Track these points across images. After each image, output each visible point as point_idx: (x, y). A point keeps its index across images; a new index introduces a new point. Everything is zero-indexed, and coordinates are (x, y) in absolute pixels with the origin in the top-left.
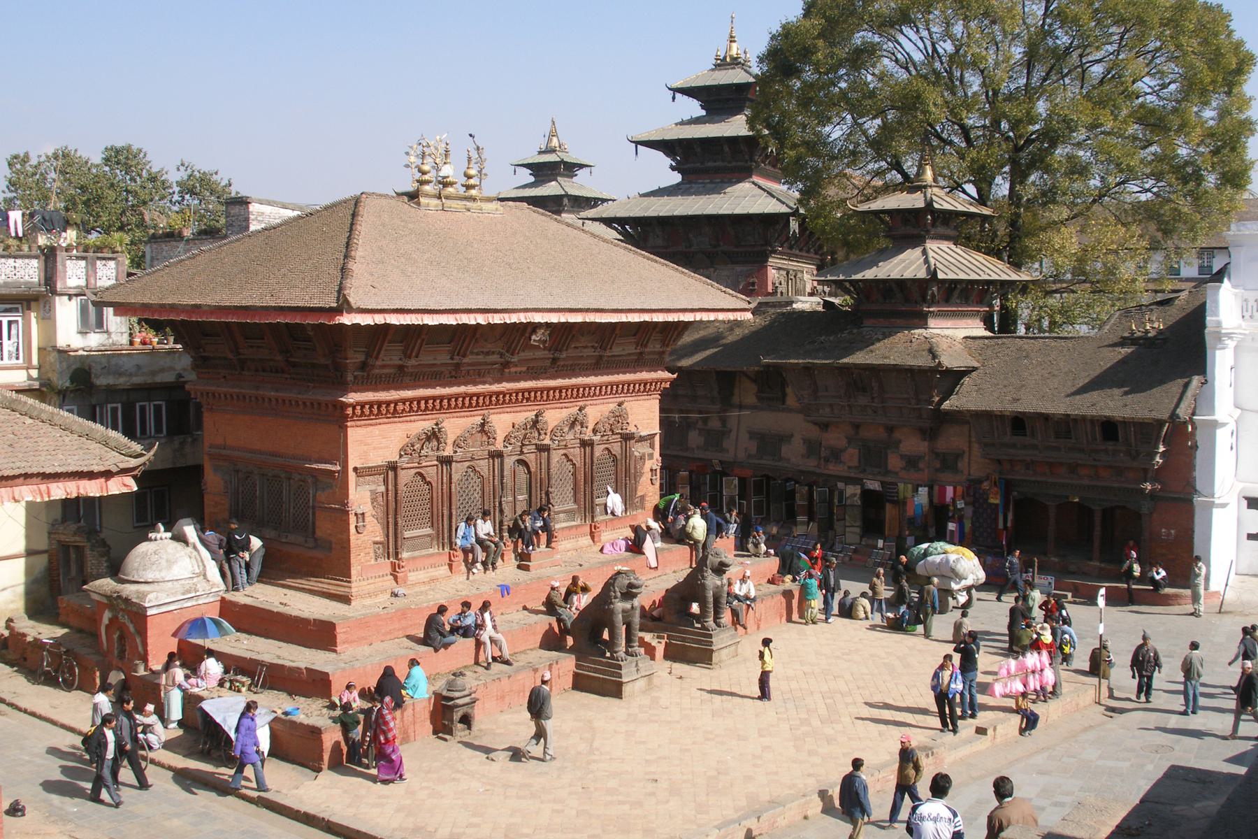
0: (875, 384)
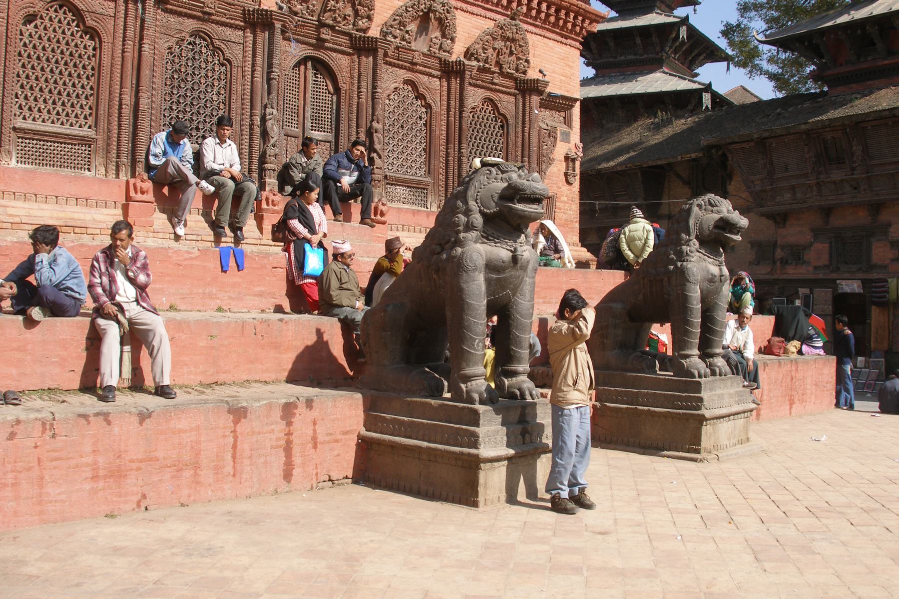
0: (857, 149)
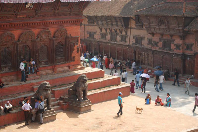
0: (166, 21)
